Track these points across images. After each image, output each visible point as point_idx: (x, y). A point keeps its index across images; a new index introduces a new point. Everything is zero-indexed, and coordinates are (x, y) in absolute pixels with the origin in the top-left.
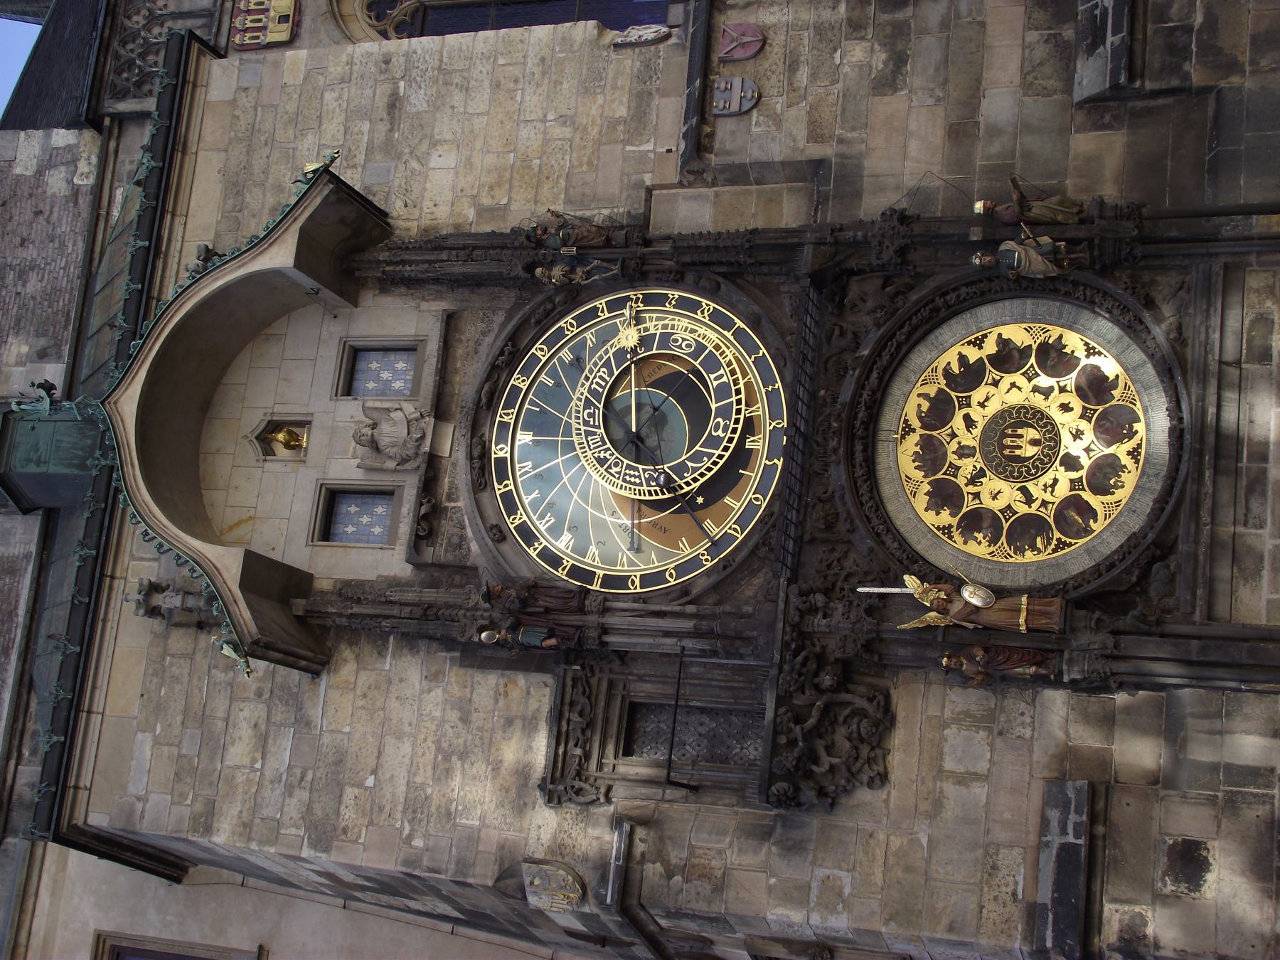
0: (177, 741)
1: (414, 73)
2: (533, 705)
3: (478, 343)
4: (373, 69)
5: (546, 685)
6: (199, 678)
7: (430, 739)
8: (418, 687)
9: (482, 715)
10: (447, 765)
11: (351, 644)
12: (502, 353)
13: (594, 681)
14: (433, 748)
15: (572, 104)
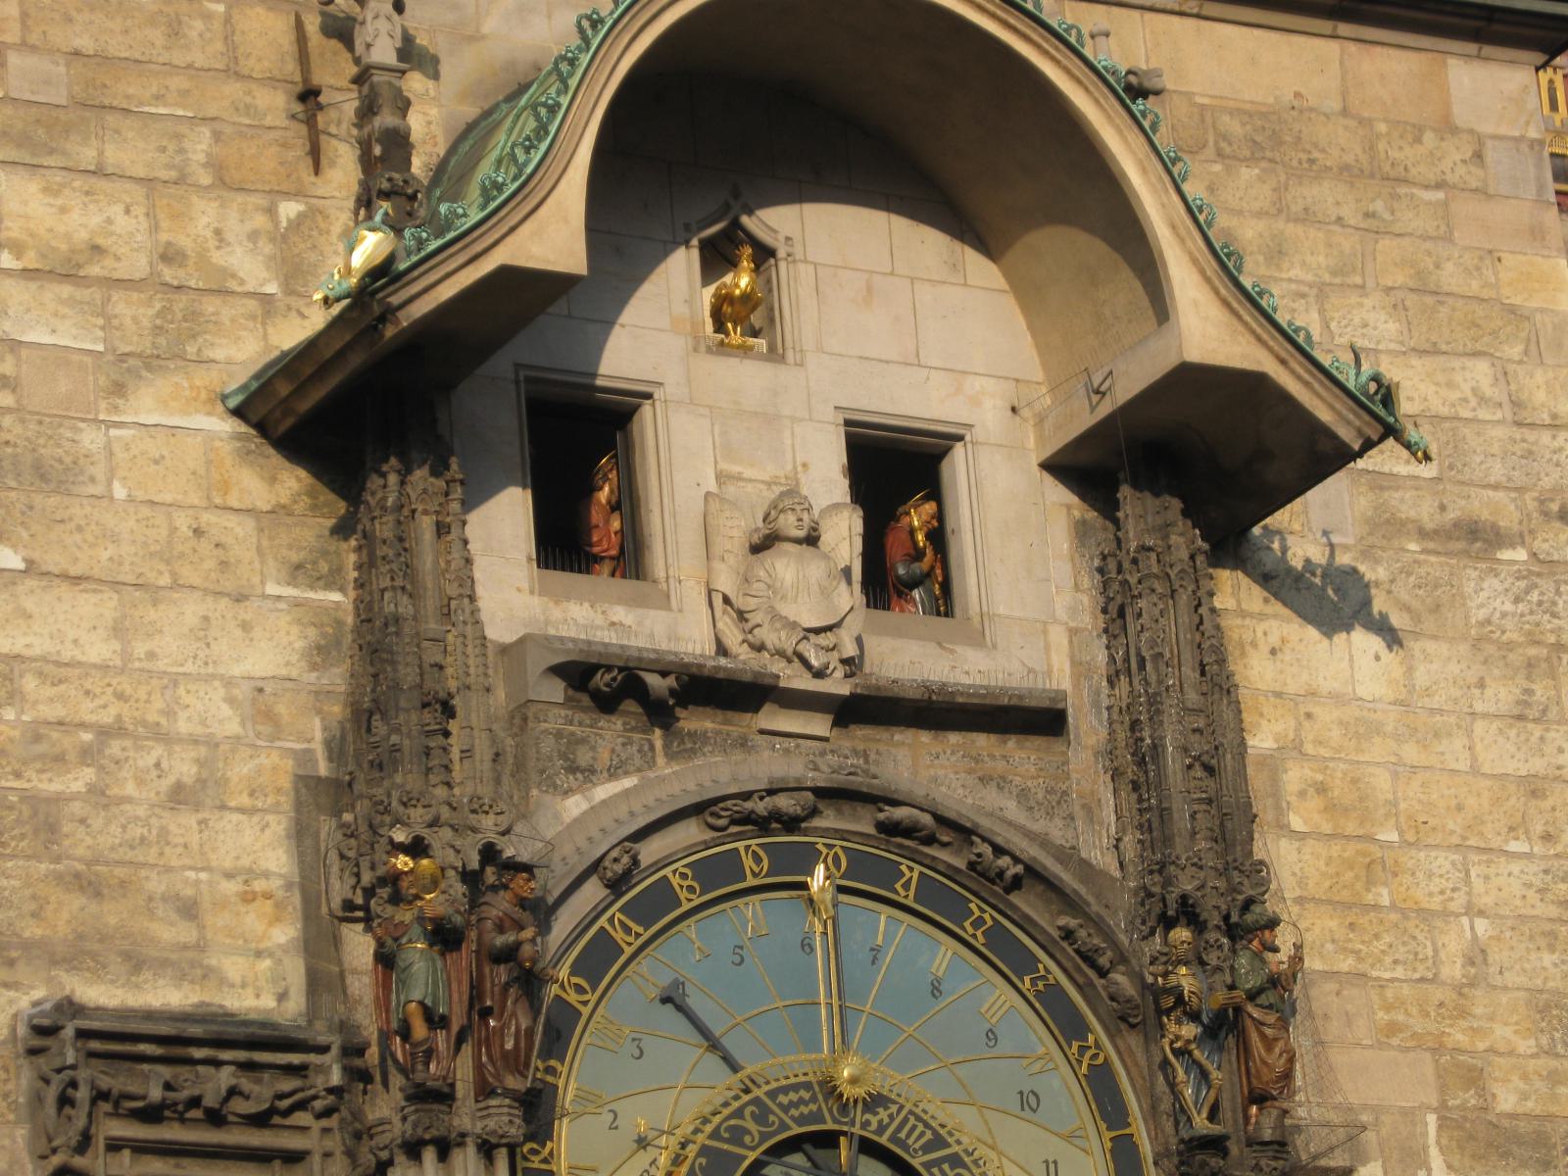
0: (34, 38)
1: (1546, 585)
2: (234, 967)
3: (1002, 783)
4: (1547, 482)
5: (282, 997)
6: (184, 93)
7: (126, 711)
8: (237, 671)
9: (194, 839)
10: (72, 756)
11: (311, 493)
12: (999, 850)
13: (302, 1118)
14: (107, 717)
15: (1512, 978)
